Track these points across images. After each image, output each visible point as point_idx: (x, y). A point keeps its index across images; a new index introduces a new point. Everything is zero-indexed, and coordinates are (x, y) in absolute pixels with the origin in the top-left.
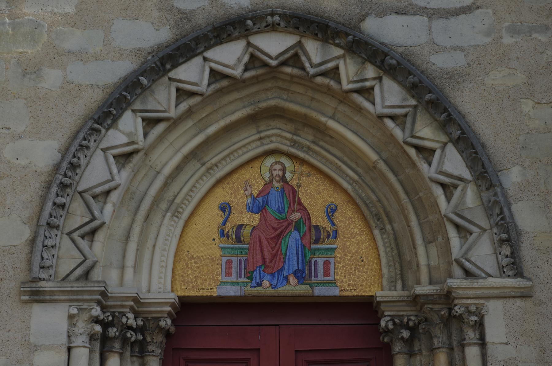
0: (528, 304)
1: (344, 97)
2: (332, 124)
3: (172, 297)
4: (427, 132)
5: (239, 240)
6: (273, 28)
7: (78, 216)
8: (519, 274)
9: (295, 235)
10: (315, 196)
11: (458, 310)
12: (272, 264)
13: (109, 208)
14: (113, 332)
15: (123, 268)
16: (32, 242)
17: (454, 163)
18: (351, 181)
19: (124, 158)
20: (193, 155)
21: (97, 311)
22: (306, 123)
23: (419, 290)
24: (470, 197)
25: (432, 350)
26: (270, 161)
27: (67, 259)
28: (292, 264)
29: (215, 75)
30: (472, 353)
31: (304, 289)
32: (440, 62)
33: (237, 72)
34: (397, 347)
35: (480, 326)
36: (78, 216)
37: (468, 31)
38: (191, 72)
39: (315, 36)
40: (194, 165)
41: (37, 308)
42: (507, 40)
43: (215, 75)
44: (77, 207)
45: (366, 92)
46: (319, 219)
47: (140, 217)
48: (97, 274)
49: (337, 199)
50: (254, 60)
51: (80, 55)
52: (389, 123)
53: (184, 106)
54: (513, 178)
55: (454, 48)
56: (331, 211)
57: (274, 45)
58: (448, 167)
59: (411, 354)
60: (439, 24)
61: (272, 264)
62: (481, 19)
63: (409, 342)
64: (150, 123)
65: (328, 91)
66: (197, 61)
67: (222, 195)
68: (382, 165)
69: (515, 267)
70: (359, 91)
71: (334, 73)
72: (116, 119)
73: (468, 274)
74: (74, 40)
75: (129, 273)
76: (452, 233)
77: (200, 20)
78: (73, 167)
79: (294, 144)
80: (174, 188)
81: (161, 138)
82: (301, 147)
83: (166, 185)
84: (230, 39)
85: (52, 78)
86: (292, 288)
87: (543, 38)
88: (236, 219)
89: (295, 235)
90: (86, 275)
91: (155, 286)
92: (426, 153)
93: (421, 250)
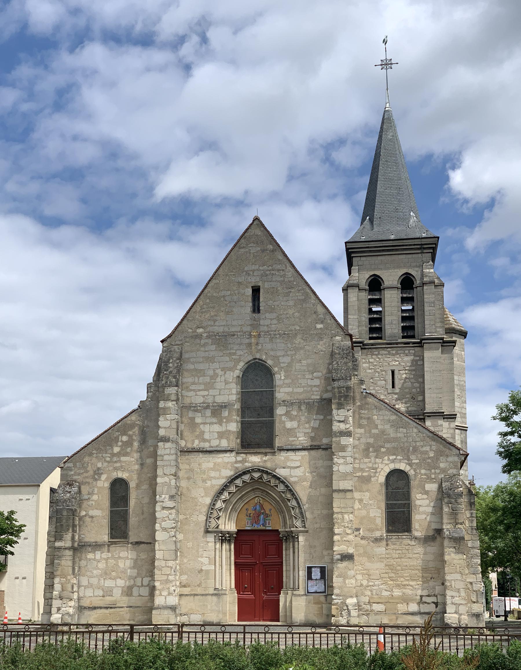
0: (307, 534)
1: (272, 486)
2: (270, 492)
3: (236, 530)
4: (289, 496)
5: (250, 517)
6: (256, 471)
7: (215, 514)
8: (305, 528)
9: (262, 516)
10: (267, 507)
11: (294, 535)
12: (257, 522)
13: (221, 513)
14: (223, 538)
15: (225, 524)
16: (207, 520)
17: (294, 503)
18: (274, 504)
19: (224, 501)
20: (240, 498)
21: (220, 535)
22: (265, 491)
23: (287, 530)
24: (297, 511)
25: (290, 542)
26: (257, 498)
27: (213, 524)
28: (261, 522)
29: (244, 482)
30: (296, 543)
31: (264, 528)
32: (292, 479)
33: (248, 481)
34: (283, 541)
35: (298, 538)
36: (215, 514)
37: (299, 472)
38: (238, 482)
39: (265, 473)
40: (240, 500)
41: (208, 535)
42: (307, 474)
43: (244, 482)
44: (215, 512)
45: (277, 486)
46: (268, 512)
47: (228, 514)
48: (220, 527)
49: (272, 508)
50: (252, 478)
51: (214, 478)
52: (282, 493)
53: (237, 489)
54: (305, 507)
55: (295, 476)
56: (270, 510)
57: (256, 475)
58: (293, 504)
59: (286, 542)
60: (292, 470)
61: (257, 522)
62: (302, 469)
63: (286, 540)
64: (230, 493)
65: (268, 485)
66: (240, 479)
67: (246, 507)
68: (280, 502)
69: (304, 527)
70: (275, 486)
71: (270, 481)
72: (222, 493)
73: (297, 527)
74: (213, 474)
75: (226, 525)
76: (294, 518)
77: (240, 469)
78: (214, 504)
79: (262, 495)
80: (236, 505)
81: (232, 496)
82: (263, 496)
83: (234, 505)
84: (247, 474)
85: (209, 483)
86: (262, 528)
87: (314, 474)
88: (249, 512)
89: (262, 516)
90: (217, 527)
91: (232, 528)
92: (289, 500)
93: (288, 521)
